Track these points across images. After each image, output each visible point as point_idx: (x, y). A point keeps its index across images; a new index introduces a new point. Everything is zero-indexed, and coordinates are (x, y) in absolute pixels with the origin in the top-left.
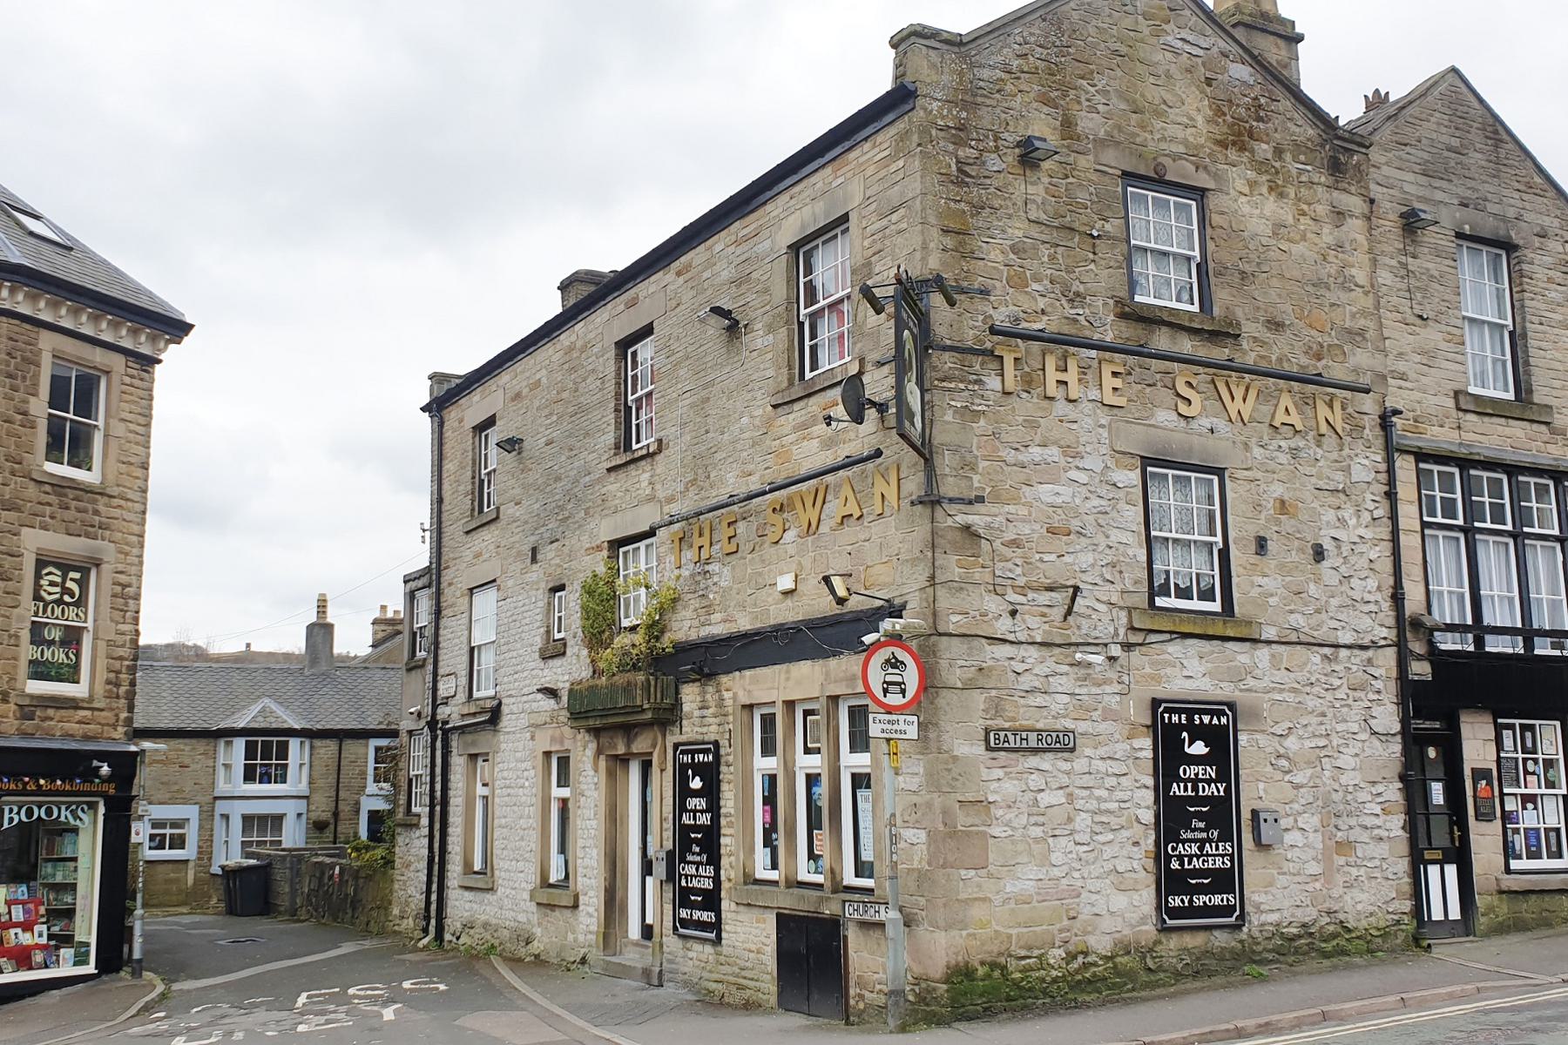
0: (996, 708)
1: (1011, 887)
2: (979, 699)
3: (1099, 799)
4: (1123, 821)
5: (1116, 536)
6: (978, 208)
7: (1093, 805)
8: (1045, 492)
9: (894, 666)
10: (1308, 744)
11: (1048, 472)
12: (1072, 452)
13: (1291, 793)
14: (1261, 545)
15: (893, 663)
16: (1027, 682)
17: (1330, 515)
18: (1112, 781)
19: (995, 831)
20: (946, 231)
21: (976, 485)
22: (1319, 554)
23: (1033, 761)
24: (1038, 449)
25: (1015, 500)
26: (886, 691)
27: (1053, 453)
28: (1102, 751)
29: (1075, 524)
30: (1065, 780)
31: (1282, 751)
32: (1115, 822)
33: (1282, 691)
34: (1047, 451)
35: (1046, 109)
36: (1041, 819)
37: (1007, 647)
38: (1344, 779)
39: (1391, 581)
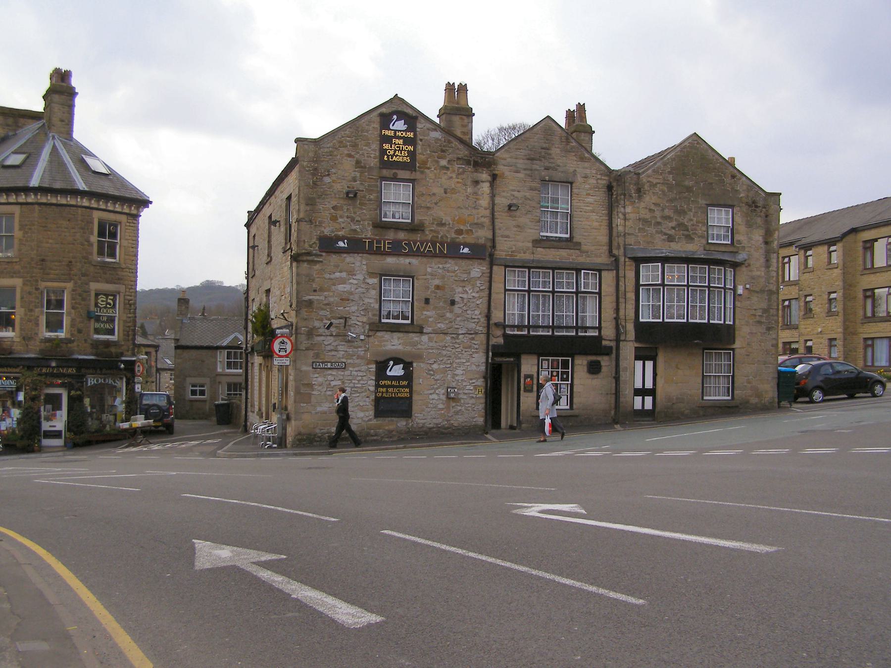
0: (317, 355)
1: (319, 409)
2: (311, 353)
3: (354, 383)
4: (363, 390)
5: (367, 300)
6: (320, 197)
7: (352, 385)
8: (341, 287)
9: (283, 343)
10: (442, 366)
11: (343, 281)
12: (351, 273)
13: (433, 382)
14: (427, 301)
15: (283, 343)
16: (329, 348)
17: (460, 289)
18: (360, 378)
19: (314, 393)
20: (307, 205)
21: (314, 286)
22: (453, 303)
23: (330, 372)
24: (339, 274)
25: (329, 290)
26: (279, 351)
27: (344, 275)
28: (357, 369)
29: (351, 297)
30: (342, 378)
31: (430, 369)
32: (359, 390)
33: (432, 349)
34: (342, 274)
35: (349, 159)
36: (331, 389)
37: (323, 337)
38: (457, 378)
39: (486, 311)
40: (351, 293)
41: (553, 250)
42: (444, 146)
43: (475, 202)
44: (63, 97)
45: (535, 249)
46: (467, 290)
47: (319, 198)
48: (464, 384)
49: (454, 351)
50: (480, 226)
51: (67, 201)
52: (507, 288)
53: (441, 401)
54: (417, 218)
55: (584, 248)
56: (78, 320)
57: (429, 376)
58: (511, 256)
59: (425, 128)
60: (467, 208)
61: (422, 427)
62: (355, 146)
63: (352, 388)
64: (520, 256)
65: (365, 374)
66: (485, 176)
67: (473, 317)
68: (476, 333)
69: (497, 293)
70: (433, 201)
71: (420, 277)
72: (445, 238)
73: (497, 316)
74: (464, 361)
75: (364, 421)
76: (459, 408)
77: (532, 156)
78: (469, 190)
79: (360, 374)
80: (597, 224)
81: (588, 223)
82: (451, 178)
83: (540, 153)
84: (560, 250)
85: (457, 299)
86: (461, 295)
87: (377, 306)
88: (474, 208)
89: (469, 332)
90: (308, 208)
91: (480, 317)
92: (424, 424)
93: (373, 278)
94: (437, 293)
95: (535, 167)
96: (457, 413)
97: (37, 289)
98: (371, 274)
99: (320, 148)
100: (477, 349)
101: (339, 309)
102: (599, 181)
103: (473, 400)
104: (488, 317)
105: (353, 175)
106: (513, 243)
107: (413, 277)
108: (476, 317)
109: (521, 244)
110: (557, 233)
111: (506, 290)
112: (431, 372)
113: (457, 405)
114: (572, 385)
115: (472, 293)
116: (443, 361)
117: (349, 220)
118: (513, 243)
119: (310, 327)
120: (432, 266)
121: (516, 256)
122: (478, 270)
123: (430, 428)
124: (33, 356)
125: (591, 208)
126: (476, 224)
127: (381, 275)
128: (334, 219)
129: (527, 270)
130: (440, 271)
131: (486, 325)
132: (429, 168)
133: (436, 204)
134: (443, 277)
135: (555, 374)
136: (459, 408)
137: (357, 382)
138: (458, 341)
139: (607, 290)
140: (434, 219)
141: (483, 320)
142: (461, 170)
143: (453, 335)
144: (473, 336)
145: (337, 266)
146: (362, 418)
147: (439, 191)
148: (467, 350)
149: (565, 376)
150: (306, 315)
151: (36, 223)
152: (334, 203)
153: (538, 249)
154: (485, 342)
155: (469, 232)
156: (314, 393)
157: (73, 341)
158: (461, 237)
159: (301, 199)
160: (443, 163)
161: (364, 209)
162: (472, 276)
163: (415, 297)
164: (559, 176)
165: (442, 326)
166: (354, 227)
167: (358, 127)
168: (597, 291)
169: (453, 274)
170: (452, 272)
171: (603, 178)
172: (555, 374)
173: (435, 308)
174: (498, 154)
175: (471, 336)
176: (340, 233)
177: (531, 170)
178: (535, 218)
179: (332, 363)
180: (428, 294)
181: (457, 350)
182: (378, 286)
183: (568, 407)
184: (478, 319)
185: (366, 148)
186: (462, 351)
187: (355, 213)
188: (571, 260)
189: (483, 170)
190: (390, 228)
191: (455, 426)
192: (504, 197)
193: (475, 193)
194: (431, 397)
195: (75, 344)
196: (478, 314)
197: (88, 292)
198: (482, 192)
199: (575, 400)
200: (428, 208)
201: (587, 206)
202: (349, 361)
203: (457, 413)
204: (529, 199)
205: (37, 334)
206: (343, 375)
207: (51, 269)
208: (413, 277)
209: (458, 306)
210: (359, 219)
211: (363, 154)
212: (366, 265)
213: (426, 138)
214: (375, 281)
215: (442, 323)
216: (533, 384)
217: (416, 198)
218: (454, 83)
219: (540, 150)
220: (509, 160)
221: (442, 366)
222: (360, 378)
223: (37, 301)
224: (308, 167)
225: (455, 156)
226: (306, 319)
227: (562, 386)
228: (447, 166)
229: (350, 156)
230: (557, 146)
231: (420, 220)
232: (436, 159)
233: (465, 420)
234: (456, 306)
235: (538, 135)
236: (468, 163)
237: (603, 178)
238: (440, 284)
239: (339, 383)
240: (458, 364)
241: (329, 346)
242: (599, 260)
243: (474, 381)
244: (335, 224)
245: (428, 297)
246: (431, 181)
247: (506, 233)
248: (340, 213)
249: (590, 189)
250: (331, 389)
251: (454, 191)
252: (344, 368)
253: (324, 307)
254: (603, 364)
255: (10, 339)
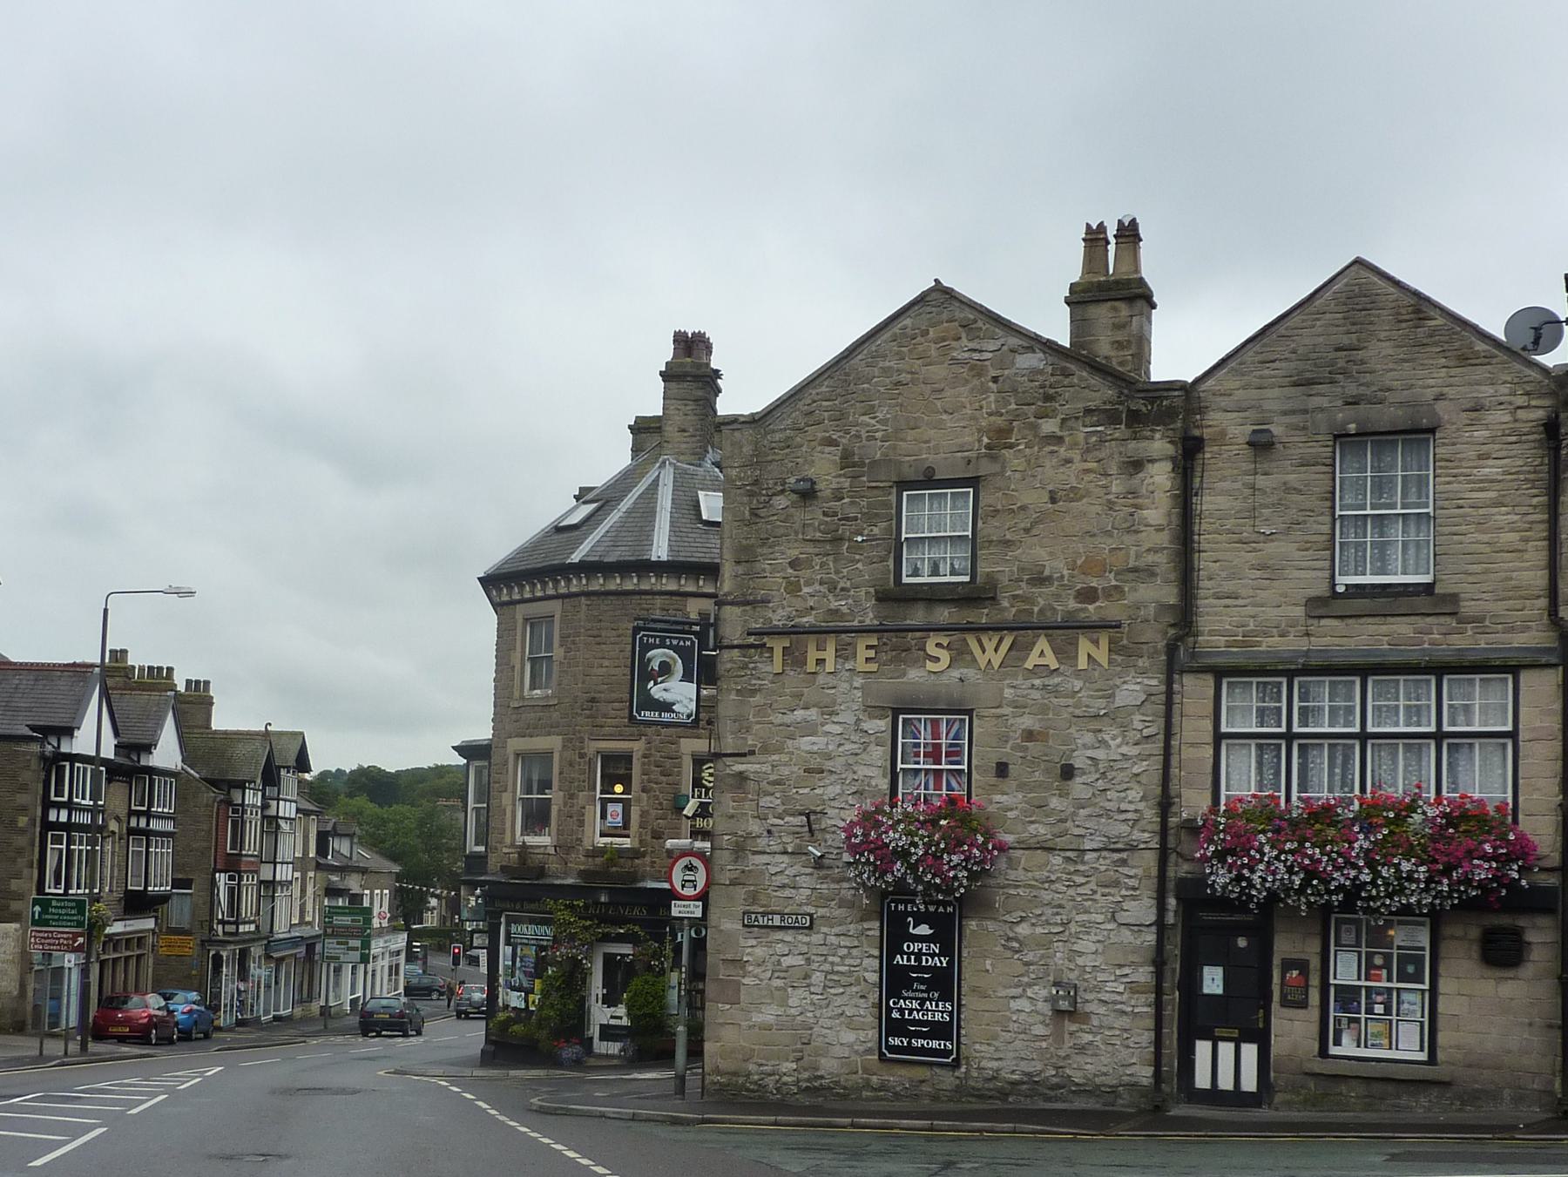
0: (753, 898)
1: (757, 1018)
2: (740, 892)
3: (832, 964)
4: (852, 980)
5: (862, 771)
6: (764, 542)
7: (827, 967)
8: (805, 743)
9: (690, 870)
10: (1039, 930)
11: (810, 729)
12: (829, 710)
13: (1023, 969)
14: (1002, 770)
15: (690, 868)
16: (779, 880)
17: (1089, 738)
18: (845, 951)
19: (746, 981)
20: (738, 563)
21: (750, 742)
22: (1068, 772)
23: (779, 935)
24: (802, 712)
25: (779, 750)
26: (683, 886)
27: (813, 714)
28: (836, 930)
29: (828, 765)
30: (805, 949)
31: (1011, 935)
32: (844, 980)
33: (1017, 887)
34: (808, 712)
35: (828, 449)
36: (782, 975)
37: (766, 856)
38: (1080, 961)
39: (1159, 791)
40: (829, 757)
41: (1370, 620)
42: (1051, 387)
43: (1132, 515)
44: (685, 385)
45: (1310, 621)
46: (1107, 737)
47: (763, 545)
48: (1101, 977)
49: (1071, 892)
50: (1141, 575)
51: (698, 587)
52: (1224, 729)
53: (1041, 1018)
54: (983, 568)
55: (1468, 608)
56: (653, 813)
57: (1009, 954)
58: (1244, 644)
59: (1005, 348)
60: (1108, 534)
61: (994, 1078)
62: (840, 417)
63: (827, 973)
64: (1272, 644)
65: (856, 944)
66: (1159, 445)
67: (1123, 806)
68: (1132, 848)
69: (1192, 745)
70: (1023, 525)
71: (986, 712)
72: (1049, 614)
73: (1194, 802)
74: (1100, 918)
75: (856, 1052)
76: (1089, 1037)
77: (1308, 375)
78: (1117, 486)
79: (845, 942)
80: (1514, 536)
81: (1485, 538)
82: (1068, 461)
83: (1332, 363)
84: (1390, 619)
85: (1079, 762)
86: (1090, 753)
87: (884, 784)
88: (1129, 531)
89: (1112, 846)
90: (740, 569)
91: (1141, 806)
92: (998, 1070)
93: (876, 718)
94: (1027, 748)
95: (1316, 401)
96: (1081, 1049)
97: (582, 756)
98: (873, 710)
99: (766, 433)
100: (1134, 889)
101: (801, 791)
102: (1521, 414)
103: (1125, 1018)
104: (1165, 804)
105: (834, 486)
106: (1250, 610)
107: (969, 712)
108: (1132, 807)
109: (1271, 613)
110: (1364, 574)
111: (1219, 737)
112: (1016, 946)
113: (1082, 1031)
114: (1434, 991)
115: (1119, 746)
116: (1044, 918)
117: (823, 589)
118: (1250, 610)
119: (740, 833)
120: (1015, 683)
121: (1259, 644)
122: (1137, 687)
123: (1014, 1083)
124: (570, 881)
125: (1492, 494)
126: (1135, 570)
127: (896, 712)
128: (793, 588)
129: (1284, 680)
130: (1036, 695)
131: (1157, 828)
132: (1011, 446)
133: (1027, 531)
134: (1044, 710)
135: (1378, 961)
136: (1089, 1037)
137: (839, 959)
138: (1082, 868)
139: (1538, 724)
140: (1021, 570)
141: (1150, 814)
142: (1094, 439)
143: (1069, 854)
144: (1124, 855)
145: (800, 696)
146: (851, 1046)
147: (1035, 498)
148: (1107, 890)
149: (1411, 969)
150: (733, 808)
151: (582, 630)
152: (794, 553)
153: (1324, 622)
154: (1154, 872)
155: (1115, 592)
156: (746, 981)
157: (643, 855)
158: (1091, 607)
159: (725, 550)
160: (1049, 426)
161: (858, 561)
162: (1119, 702)
163: (974, 762)
164: (1387, 415)
165: (1041, 830)
166: (834, 604)
167: (847, 375)
168: (1509, 728)
169: (1070, 701)
170: (1066, 696)
171: (1533, 403)
172: (1378, 961)
173: (1022, 787)
174: (1203, 387)
175: (1116, 856)
176: (805, 620)
177: (1305, 411)
178: (1315, 538)
179: (782, 914)
180: (1007, 752)
181: (1080, 890)
182: (888, 736)
183: (1423, 1056)
184: (1136, 811)
185: (866, 418)
186: (1095, 892)
187: (837, 572)
188: (1426, 646)
189: (1153, 431)
190: (915, 600)
191: (1077, 1084)
192: (1223, 493)
193: (1133, 493)
194: (1014, 1005)
195: (648, 859)
196: (1137, 799)
197: (676, 757)
198: (1151, 488)
199: (1442, 1038)
200: (1007, 543)
201: (1481, 490)
202: (821, 911)
203: (1081, 1049)
204: (1299, 492)
205: (580, 840)
206: (808, 944)
207: (605, 716)
208: (969, 712)
209: (1084, 779)
210: (848, 584)
211: (858, 436)
212: (862, 688)
213: (1006, 372)
214: (883, 724)
215: (1039, 823)
216: (1307, 986)
217: (980, 524)
218: (1101, 225)
219: (1333, 355)
220: (1240, 394)
221: (1039, 930)
222: (845, 951)
223: (582, 777)
224: (740, 479)
225: (1081, 405)
226: (732, 817)
227: (1405, 996)
228: (1059, 434)
229: (831, 442)
230: (1383, 335)
231: (988, 574)
232: (1032, 419)
233: (1104, 1069)
234: (1078, 780)
235: (1328, 316)
236: (1112, 418)
237: (1533, 403)
238: (1037, 727)
239: (800, 961)
240: (1084, 926)
241: (778, 878)
242: (1520, 640)
243: (1126, 971)
244: (794, 600)
245: (1004, 760)
246: (1018, 475)
247: (1228, 587)
248: (806, 573)
249: (1493, 440)
250: (782, 975)
251: (1074, 494)
252: (810, 928)
253: (770, 789)
254: (1531, 936)
255: (542, 850)
